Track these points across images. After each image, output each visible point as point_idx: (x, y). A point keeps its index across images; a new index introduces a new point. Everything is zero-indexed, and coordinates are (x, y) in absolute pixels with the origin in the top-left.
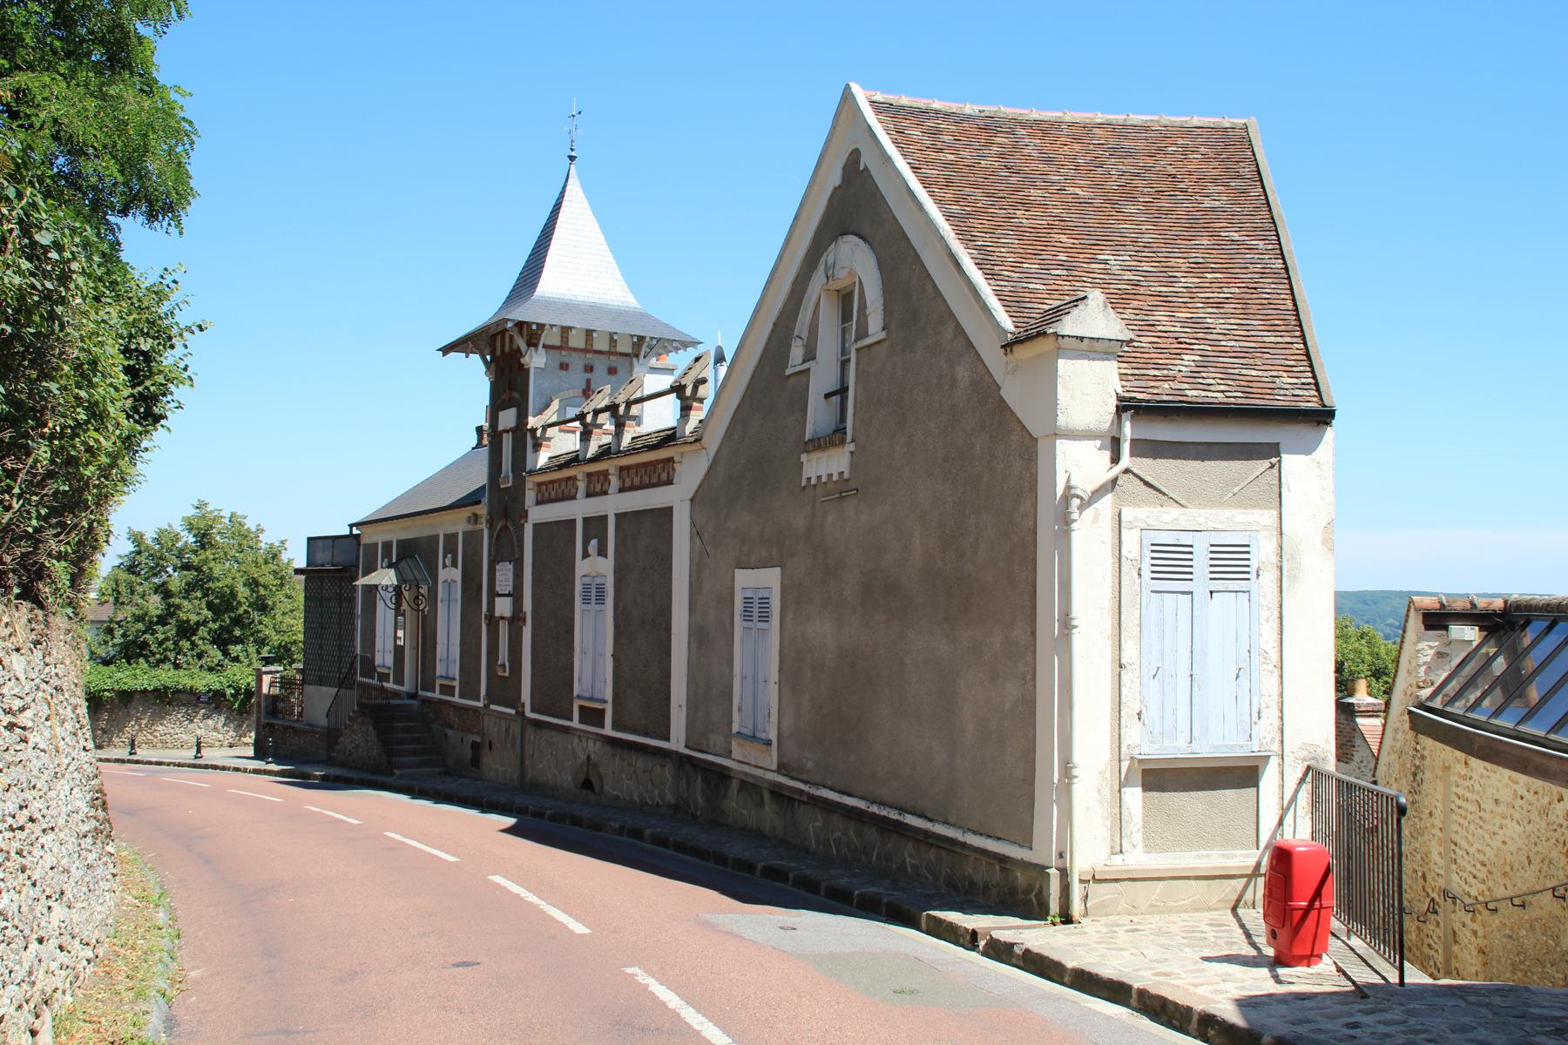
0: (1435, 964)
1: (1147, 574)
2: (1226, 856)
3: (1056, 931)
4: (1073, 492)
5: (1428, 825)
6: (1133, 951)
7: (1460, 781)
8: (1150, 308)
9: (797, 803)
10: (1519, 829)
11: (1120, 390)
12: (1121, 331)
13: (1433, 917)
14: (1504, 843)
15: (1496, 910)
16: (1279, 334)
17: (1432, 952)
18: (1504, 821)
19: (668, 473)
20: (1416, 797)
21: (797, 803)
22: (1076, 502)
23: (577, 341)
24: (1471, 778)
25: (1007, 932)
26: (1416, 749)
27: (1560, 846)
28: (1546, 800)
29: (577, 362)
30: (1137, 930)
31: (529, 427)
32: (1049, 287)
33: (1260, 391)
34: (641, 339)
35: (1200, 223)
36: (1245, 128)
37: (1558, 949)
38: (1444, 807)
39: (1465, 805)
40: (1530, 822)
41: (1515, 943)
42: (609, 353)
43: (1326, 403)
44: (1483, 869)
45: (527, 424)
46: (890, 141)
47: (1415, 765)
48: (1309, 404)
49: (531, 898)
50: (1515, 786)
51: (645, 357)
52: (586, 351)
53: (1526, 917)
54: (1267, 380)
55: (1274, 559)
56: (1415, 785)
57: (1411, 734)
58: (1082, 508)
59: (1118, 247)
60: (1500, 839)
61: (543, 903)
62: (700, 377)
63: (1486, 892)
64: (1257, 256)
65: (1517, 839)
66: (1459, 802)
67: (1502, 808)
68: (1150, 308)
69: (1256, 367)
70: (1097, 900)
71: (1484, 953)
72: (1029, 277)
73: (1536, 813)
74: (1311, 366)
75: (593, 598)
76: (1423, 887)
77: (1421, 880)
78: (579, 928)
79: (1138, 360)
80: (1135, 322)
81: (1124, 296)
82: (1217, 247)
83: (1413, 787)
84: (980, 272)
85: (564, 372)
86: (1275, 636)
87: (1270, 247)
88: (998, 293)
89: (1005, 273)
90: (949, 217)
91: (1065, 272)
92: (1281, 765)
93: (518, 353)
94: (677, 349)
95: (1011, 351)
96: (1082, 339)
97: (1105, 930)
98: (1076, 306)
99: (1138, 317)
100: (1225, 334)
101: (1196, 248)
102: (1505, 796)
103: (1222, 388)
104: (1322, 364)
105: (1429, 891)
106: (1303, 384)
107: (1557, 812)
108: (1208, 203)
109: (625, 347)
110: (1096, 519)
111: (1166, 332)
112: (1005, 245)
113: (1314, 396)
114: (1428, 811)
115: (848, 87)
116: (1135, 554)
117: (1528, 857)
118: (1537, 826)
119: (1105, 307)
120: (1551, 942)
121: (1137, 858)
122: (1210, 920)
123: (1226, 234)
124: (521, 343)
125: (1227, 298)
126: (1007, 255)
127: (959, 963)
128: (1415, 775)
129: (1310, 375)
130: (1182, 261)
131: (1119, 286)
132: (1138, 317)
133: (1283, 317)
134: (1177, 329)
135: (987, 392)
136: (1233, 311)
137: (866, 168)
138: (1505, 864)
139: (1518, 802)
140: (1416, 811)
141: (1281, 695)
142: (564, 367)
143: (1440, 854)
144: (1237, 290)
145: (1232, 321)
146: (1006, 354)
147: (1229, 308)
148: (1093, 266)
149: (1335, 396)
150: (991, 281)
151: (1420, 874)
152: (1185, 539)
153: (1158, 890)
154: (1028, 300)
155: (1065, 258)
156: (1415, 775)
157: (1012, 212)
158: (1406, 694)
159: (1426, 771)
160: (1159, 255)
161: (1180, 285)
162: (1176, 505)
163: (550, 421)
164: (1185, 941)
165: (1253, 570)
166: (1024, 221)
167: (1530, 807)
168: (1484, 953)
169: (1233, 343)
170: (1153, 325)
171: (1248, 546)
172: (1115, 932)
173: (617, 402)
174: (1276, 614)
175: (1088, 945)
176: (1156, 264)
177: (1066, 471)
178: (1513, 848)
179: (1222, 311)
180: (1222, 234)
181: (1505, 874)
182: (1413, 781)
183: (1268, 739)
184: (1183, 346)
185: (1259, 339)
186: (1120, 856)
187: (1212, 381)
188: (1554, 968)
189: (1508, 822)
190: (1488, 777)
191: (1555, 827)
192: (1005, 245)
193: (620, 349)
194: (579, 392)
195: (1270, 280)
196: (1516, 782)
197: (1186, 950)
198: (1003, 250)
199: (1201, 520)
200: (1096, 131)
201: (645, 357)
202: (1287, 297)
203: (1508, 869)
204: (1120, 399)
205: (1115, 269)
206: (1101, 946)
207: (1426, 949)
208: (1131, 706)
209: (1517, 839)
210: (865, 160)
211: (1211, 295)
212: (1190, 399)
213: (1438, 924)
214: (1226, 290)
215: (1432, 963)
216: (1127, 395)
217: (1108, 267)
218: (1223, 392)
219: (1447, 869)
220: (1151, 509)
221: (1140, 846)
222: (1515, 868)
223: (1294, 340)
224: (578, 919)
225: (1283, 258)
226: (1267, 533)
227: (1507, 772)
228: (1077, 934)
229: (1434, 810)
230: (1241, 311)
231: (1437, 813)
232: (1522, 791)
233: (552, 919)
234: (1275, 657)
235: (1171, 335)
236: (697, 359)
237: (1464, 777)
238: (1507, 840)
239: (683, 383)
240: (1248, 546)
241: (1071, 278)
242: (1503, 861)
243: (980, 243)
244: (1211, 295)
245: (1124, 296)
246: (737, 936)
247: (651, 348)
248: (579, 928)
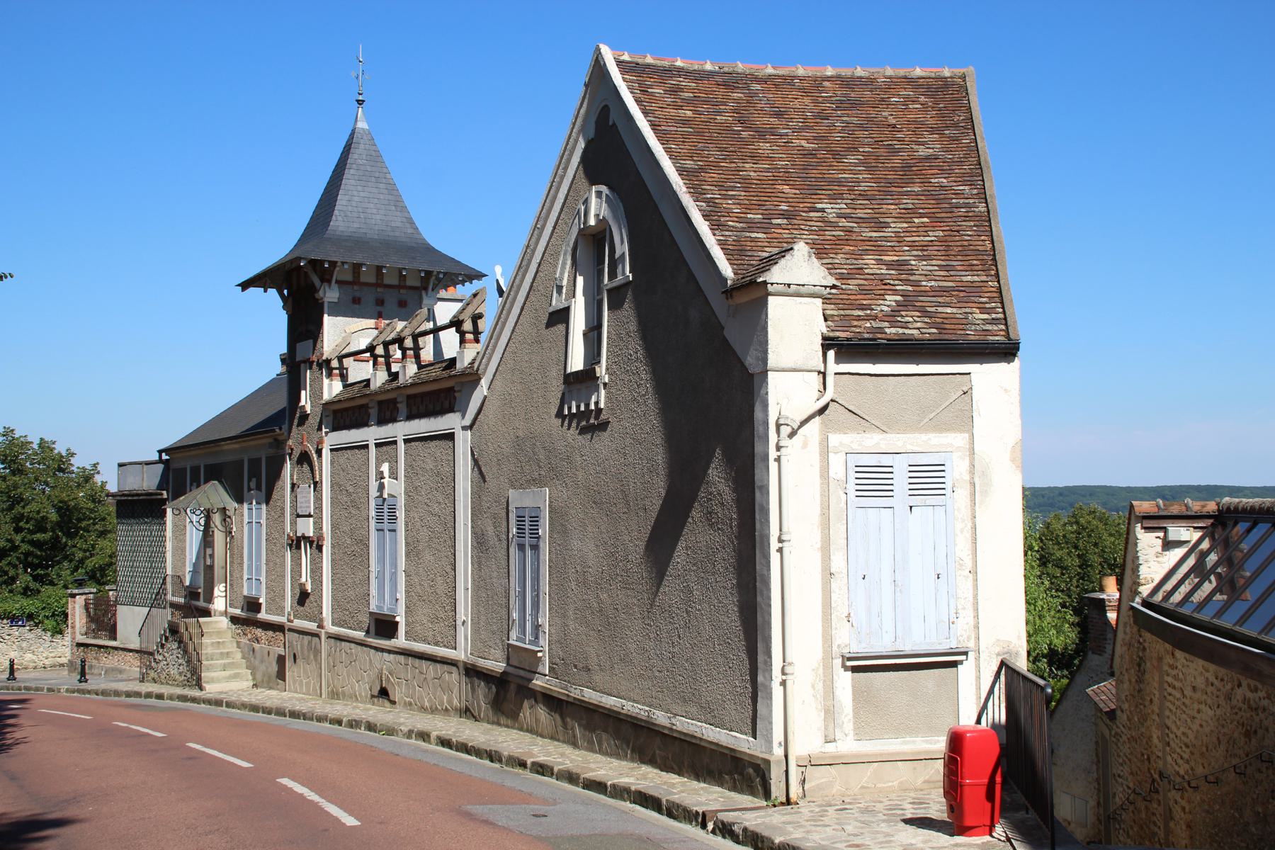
0: (1159, 839)
1: (852, 493)
2: (927, 742)
3: (775, 812)
4: (781, 421)
5: (1150, 711)
6: (837, 827)
7: (1170, 671)
8: (860, 252)
9: (565, 703)
10: (1211, 713)
11: (825, 330)
12: (824, 278)
13: (1155, 796)
14: (1201, 726)
15: (1197, 787)
16: (975, 273)
17: (1156, 829)
18: (1200, 706)
19: (450, 402)
20: (1141, 685)
21: (565, 703)
22: (785, 431)
23: (367, 276)
24: (1176, 668)
25: (731, 813)
26: (1139, 642)
27: (1240, 727)
28: (1229, 686)
30: (846, 809)
31: (324, 358)
32: (769, 236)
33: (953, 327)
34: (429, 273)
35: (910, 171)
36: (964, 77)
37: (1242, 821)
38: (1160, 694)
39: (1173, 692)
40: (1218, 707)
41: (1211, 817)
42: (399, 287)
43: (1012, 336)
44: (1188, 751)
45: (322, 354)
46: (633, 99)
47: (1139, 656)
48: (997, 338)
49: (313, 797)
50: (1207, 675)
51: (433, 290)
52: (377, 285)
53: (1219, 793)
54: (961, 316)
55: (967, 478)
56: (1140, 674)
57: (1135, 629)
58: (792, 434)
59: (834, 198)
60: (1198, 722)
61: (323, 800)
62: (476, 312)
63: (1190, 772)
64: (962, 201)
65: (1210, 722)
66: (1170, 690)
67: (1198, 695)
68: (860, 252)
69: (952, 305)
70: (813, 784)
71: (1190, 827)
72: (752, 226)
73: (1223, 698)
74: (1002, 303)
75: (386, 517)
76: (1149, 769)
77: (1146, 762)
78: (350, 821)
79: (845, 302)
80: (845, 267)
81: (837, 242)
82: (927, 194)
83: (1138, 677)
84: (707, 223)
85: (357, 306)
86: (969, 545)
87: (975, 192)
88: (720, 243)
89: (730, 223)
90: (682, 171)
91: (785, 221)
92: (977, 659)
93: (314, 290)
94: (463, 283)
95: (731, 296)
96: (789, 285)
97: (817, 810)
98: (784, 256)
99: (848, 262)
100: (926, 275)
101: (907, 194)
102: (1200, 682)
103: (919, 325)
104: (1012, 301)
105: (1153, 772)
106: (993, 319)
107: (1238, 697)
108: (922, 151)
110: (805, 445)
111: (873, 274)
112: (732, 197)
113: (1001, 330)
114: (1149, 699)
115: (598, 49)
116: (841, 475)
117: (1218, 738)
118: (1224, 710)
119: (810, 257)
120: (1236, 814)
121: (847, 745)
122: (914, 799)
123: (936, 180)
125: (932, 241)
126: (733, 207)
127: (684, 842)
128: (1139, 665)
129: (1001, 310)
130: (893, 207)
131: (834, 233)
132: (848, 262)
133: (981, 257)
134: (883, 271)
135: (713, 329)
136: (936, 253)
137: (614, 124)
138: (1202, 745)
139: (1210, 689)
140: (1141, 699)
141: (975, 596)
142: (356, 301)
143: (1158, 737)
144: (941, 234)
145: (934, 262)
146: (727, 299)
147: (932, 251)
148: (812, 214)
149: (1024, 331)
150: (716, 232)
151: (1146, 757)
152: (886, 460)
153: (869, 774)
154: (749, 248)
155: (786, 208)
156: (1139, 665)
157: (741, 165)
158: (1131, 591)
159: (1147, 661)
160: (874, 202)
161: (890, 229)
162: (878, 430)
163: (344, 352)
164: (885, 817)
165: (948, 486)
166: (752, 174)
167: (1218, 693)
168: (1190, 827)
169: (933, 283)
170: (862, 269)
171: (943, 465)
172: (827, 811)
173: (403, 335)
174: (970, 525)
175: (799, 822)
176: (870, 211)
177: (778, 404)
178: (1207, 730)
179: (925, 253)
180: (933, 181)
181: (1202, 754)
182: (1139, 671)
183: (965, 636)
184: (884, 286)
185: (958, 279)
186: (834, 744)
187: (911, 319)
188: (1239, 838)
189: (1202, 707)
190: (1188, 666)
191: (1236, 710)
192: (732, 197)
193: (409, 283)
195: (972, 224)
196: (1207, 671)
197: (882, 825)
198: (730, 202)
199: (900, 444)
200: (826, 84)
201: (433, 290)
202: (986, 238)
203: (1204, 749)
204: (824, 338)
205: (832, 217)
206: (809, 823)
207: (1152, 826)
208: (840, 609)
209: (1210, 722)
210: (614, 117)
211: (917, 239)
212: (888, 337)
213: (1159, 801)
214: (930, 233)
215: (1156, 839)
216: (831, 334)
217: (825, 214)
218: (919, 329)
219: (1164, 751)
220: (855, 435)
221: (852, 733)
222: (1209, 749)
223: (990, 278)
224: (351, 813)
225: (986, 203)
226: (960, 454)
227: (1201, 662)
228: (792, 814)
229: (1153, 697)
230: (943, 253)
231: (1156, 700)
232: (1212, 679)
233: (327, 813)
234: (969, 564)
235: (877, 277)
236: (475, 295)
237: (1172, 667)
238: (1204, 724)
239: (461, 318)
240: (943, 465)
241: (790, 227)
242: (1200, 743)
243: (709, 196)
244: (917, 239)
245: (837, 242)
246: (491, 823)
247: (439, 280)
248: (350, 821)
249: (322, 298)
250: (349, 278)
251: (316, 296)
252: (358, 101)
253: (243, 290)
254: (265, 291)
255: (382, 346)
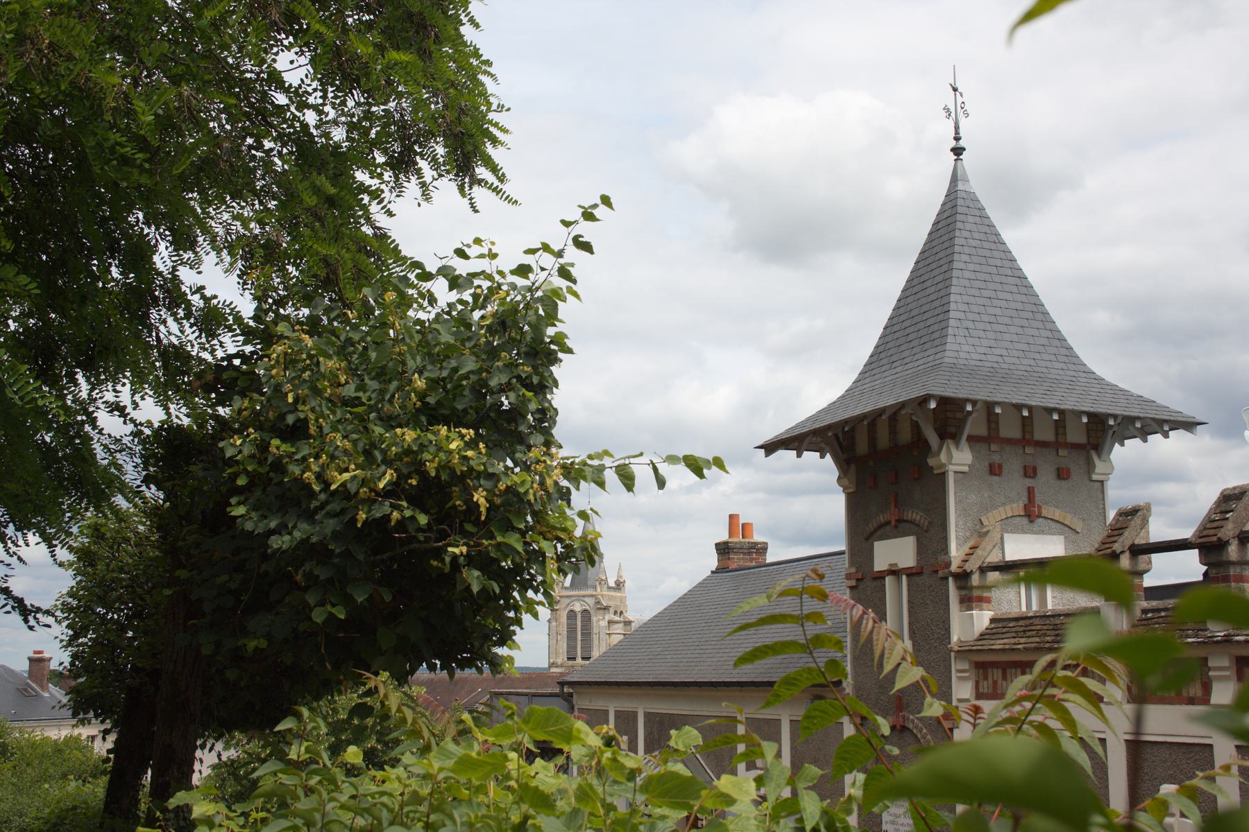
23: (1010, 430)
29: (1013, 463)
31: (954, 568)
45: (948, 564)
85: (997, 478)
94: (1144, 434)
109: (1075, 435)
124: (933, 439)
142: (995, 470)
194: (1018, 508)
249: (944, 465)
250: (982, 431)
251: (931, 462)
252: (952, 150)
253: (768, 454)
254: (799, 456)
255: (1127, 554)
